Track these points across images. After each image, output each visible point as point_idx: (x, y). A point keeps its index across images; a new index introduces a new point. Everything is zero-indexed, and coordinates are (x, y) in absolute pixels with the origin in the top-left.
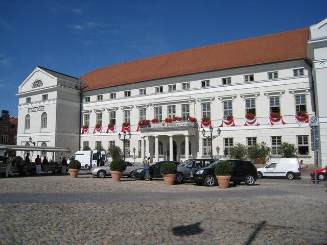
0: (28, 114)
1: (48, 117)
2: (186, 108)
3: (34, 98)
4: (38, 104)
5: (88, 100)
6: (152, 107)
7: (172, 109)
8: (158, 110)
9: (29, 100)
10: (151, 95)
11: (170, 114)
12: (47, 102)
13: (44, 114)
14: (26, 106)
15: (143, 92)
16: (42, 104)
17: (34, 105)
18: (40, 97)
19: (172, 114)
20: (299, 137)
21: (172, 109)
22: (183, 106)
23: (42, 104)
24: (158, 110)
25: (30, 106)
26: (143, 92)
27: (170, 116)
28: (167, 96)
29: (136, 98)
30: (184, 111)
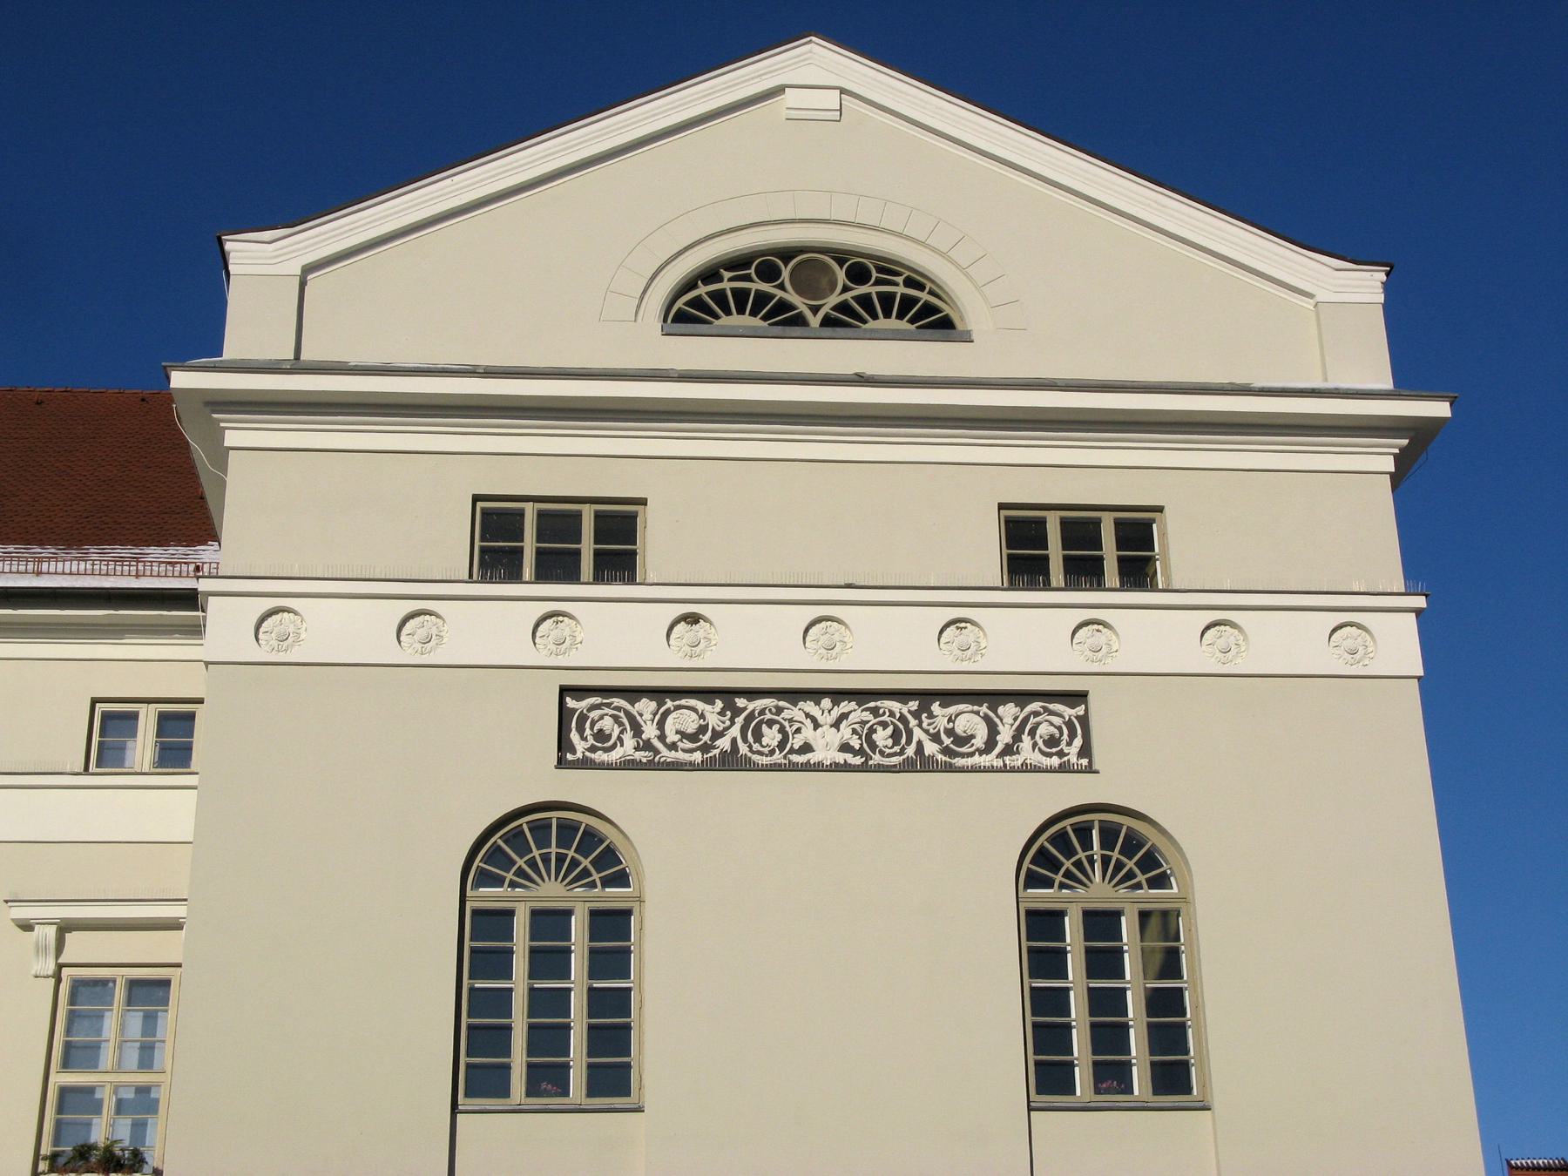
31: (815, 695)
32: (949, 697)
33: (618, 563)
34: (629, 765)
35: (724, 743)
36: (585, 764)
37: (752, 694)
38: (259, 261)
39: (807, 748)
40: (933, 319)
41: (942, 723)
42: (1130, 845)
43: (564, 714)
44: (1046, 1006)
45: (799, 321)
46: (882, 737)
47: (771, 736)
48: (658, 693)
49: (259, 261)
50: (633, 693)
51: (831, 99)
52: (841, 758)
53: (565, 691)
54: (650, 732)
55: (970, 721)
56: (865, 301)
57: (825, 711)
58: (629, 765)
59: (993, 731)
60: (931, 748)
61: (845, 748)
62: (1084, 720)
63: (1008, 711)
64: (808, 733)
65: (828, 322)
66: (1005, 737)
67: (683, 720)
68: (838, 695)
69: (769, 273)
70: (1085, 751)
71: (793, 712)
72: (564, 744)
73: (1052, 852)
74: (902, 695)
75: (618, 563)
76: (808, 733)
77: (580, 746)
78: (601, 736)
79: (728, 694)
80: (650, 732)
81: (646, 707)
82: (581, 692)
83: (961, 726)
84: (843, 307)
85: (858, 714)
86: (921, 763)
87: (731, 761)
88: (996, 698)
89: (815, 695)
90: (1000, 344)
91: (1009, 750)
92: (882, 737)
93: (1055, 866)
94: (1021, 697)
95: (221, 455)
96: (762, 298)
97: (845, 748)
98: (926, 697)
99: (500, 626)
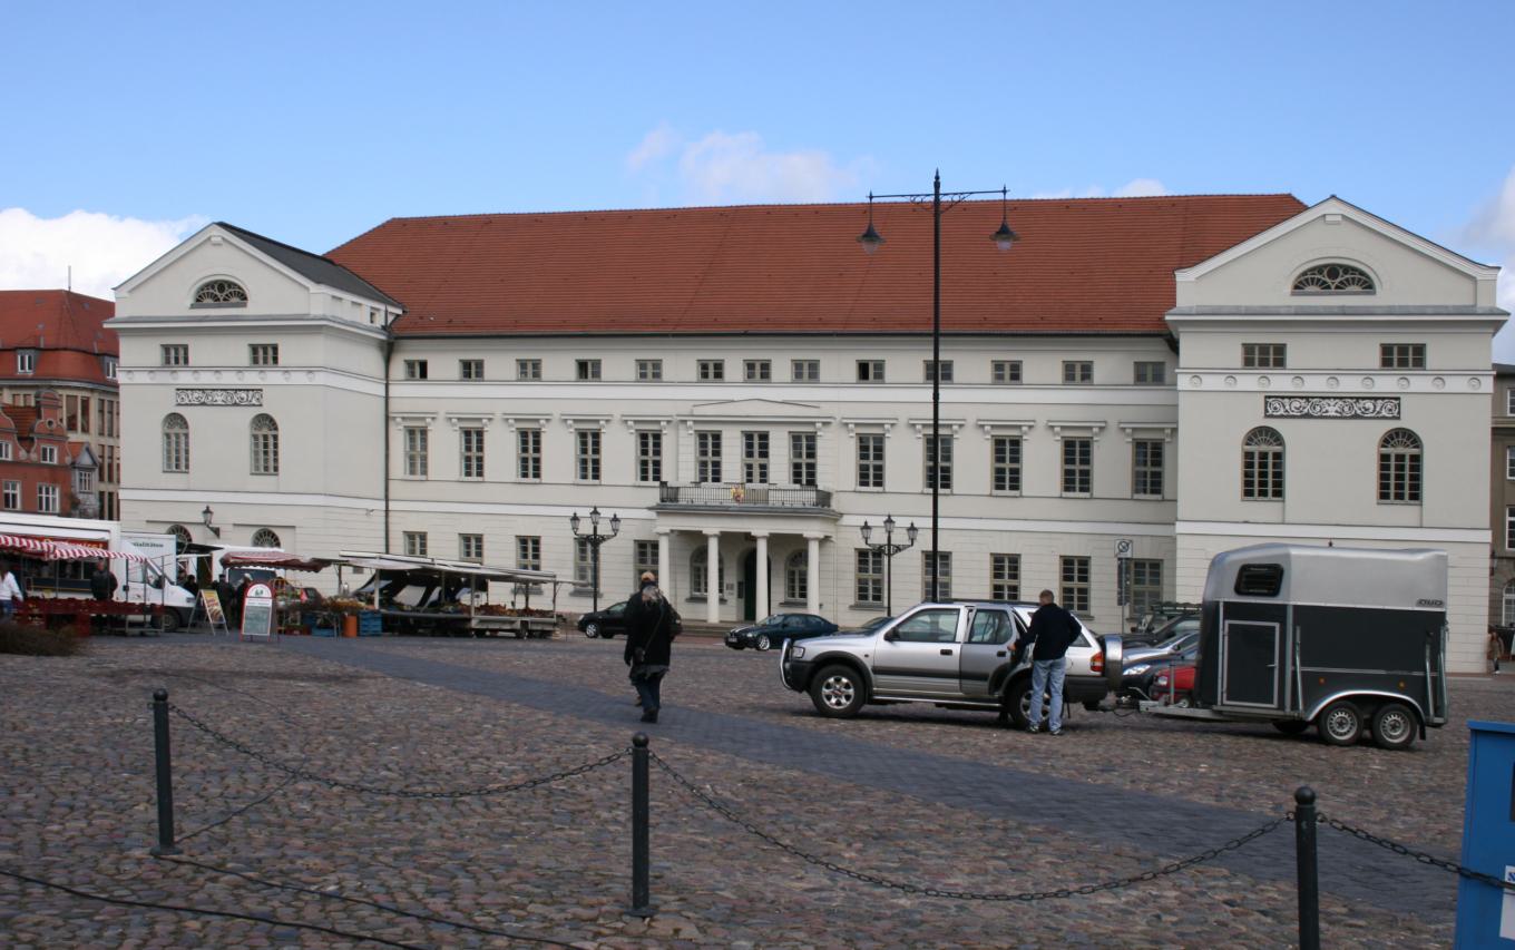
0: (181, 411)
1: (281, 433)
2: (804, 446)
3: (200, 351)
4: (229, 379)
5: (420, 371)
6: (683, 432)
7: (757, 444)
8: (710, 443)
9: (176, 356)
10: (679, 391)
11: (750, 461)
12: (272, 377)
13: (265, 422)
14: (165, 377)
15: (650, 371)
16: (252, 378)
17: (207, 379)
18: (238, 351)
19: (756, 461)
20: (1067, 562)
21: (757, 444)
22: (796, 438)
23: (252, 378)
24: (710, 443)
25: (185, 378)
26: (650, 371)
27: (750, 467)
28: (737, 398)
29: (621, 393)
30: (799, 455)
31: (1329, 398)
32: (1364, 398)
33: (1280, 364)
34: (1282, 416)
35: (1306, 411)
36: (1272, 416)
37: (1313, 398)
38: (1184, 278)
39: (1327, 411)
40: (1367, 285)
41: (1361, 406)
42: (1410, 438)
43: (1266, 403)
44: (1384, 477)
45: (1329, 287)
46: (1346, 409)
47: (1318, 408)
48: (1290, 398)
49: (1184, 278)
50: (1283, 398)
51: (1339, 218)
52: (1335, 414)
53: (1266, 397)
54: (1287, 407)
55: (1369, 404)
56: (1347, 280)
57: (1332, 402)
58: (1282, 416)
59: (1375, 407)
60: (1359, 412)
61: (1337, 412)
62: (1399, 404)
63: (1380, 402)
64: (1327, 408)
65: (1337, 287)
66: (1378, 409)
67: (1296, 404)
68: (1335, 398)
69: (1321, 272)
70: (1399, 413)
71: (1324, 402)
72: (1266, 411)
73: (1388, 439)
74: (1352, 398)
75: (1280, 364)
76: (1327, 408)
77: (1270, 412)
78: (1275, 408)
79: (1307, 398)
80: (1287, 407)
81: (1286, 400)
82: (1270, 397)
83: (1367, 406)
84: (1341, 282)
85: (1340, 403)
86: (1356, 417)
87: (1308, 416)
88: (1376, 399)
89: (1329, 398)
90: (1383, 297)
91: (1378, 413)
92: (1346, 409)
93: (1388, 443)
94: (1383, 399)
95: (1178, 334)
96: (1319, 280)
97: (1337, 412)
98: (1358, 399)
99: (1250, 381)
